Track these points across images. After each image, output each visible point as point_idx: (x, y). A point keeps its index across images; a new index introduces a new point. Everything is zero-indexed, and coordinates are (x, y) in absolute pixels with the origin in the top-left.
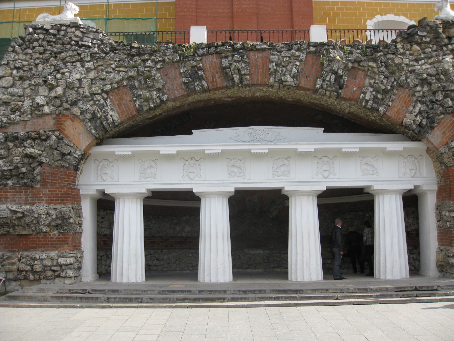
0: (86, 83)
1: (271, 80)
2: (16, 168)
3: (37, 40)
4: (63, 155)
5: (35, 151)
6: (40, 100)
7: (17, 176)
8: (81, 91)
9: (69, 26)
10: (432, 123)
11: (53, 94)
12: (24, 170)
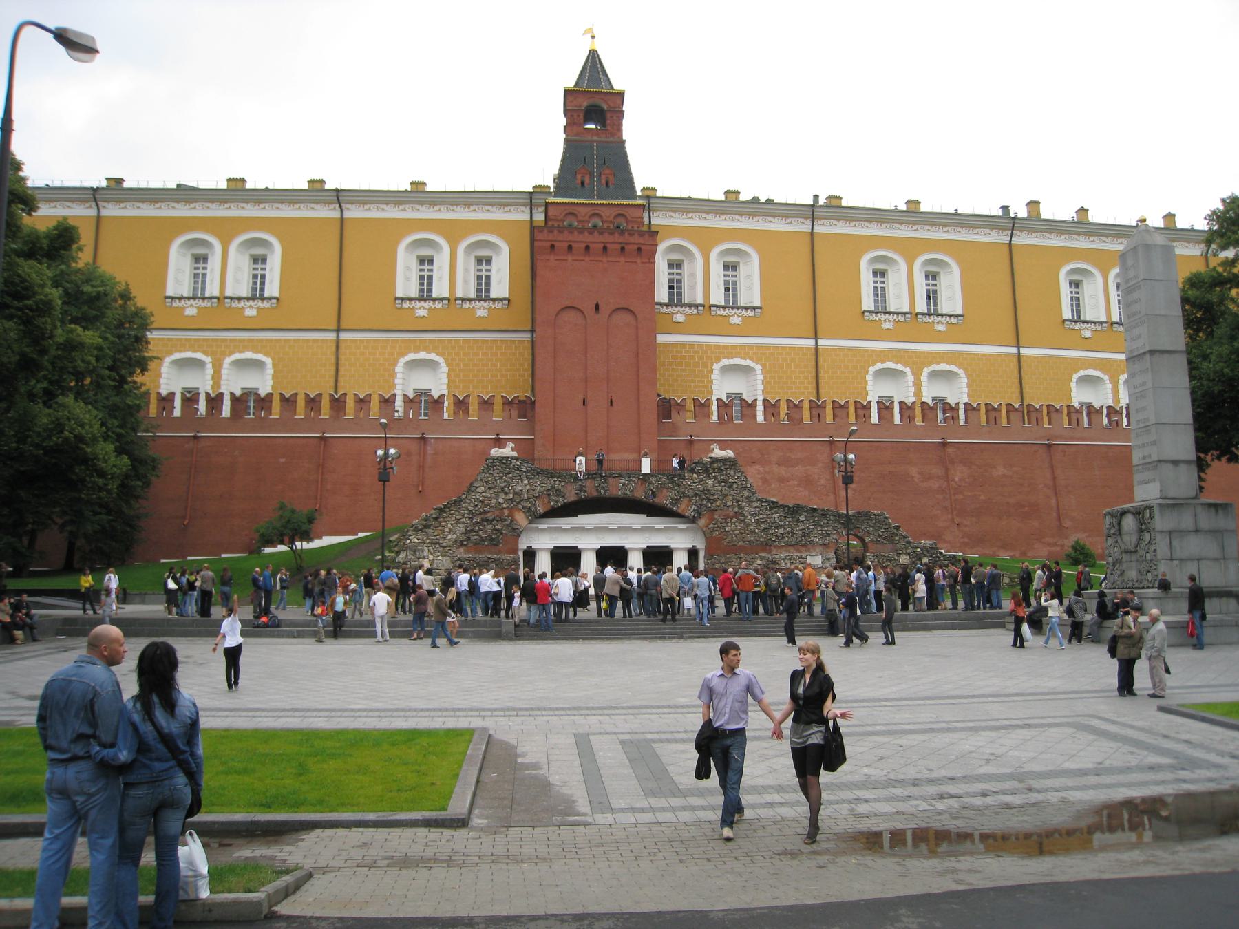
6: (501, 501)
9: (512, 458)
10: (700, 515)
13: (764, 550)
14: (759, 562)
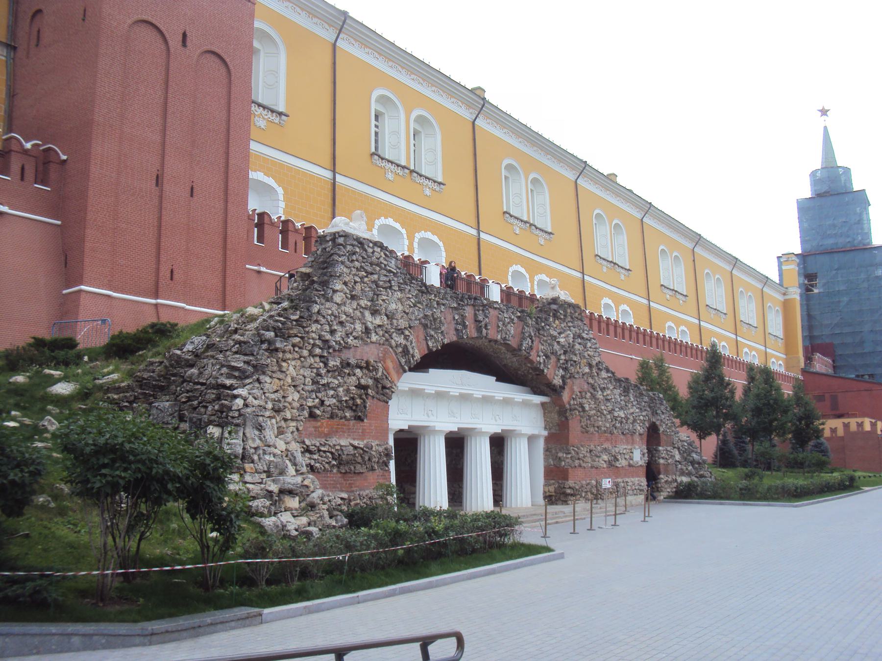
0: (399, 316)
1: (499, 337)
2: (353, 399)
3: (354, 253)
4: (384, 387)
5: (367, 381)
7: (351, 408)
8: (395, 321)
9: (376, 244)
11: (378, 321)
12: (359, 401)
13: (607, 440)
14: (605, 457)
